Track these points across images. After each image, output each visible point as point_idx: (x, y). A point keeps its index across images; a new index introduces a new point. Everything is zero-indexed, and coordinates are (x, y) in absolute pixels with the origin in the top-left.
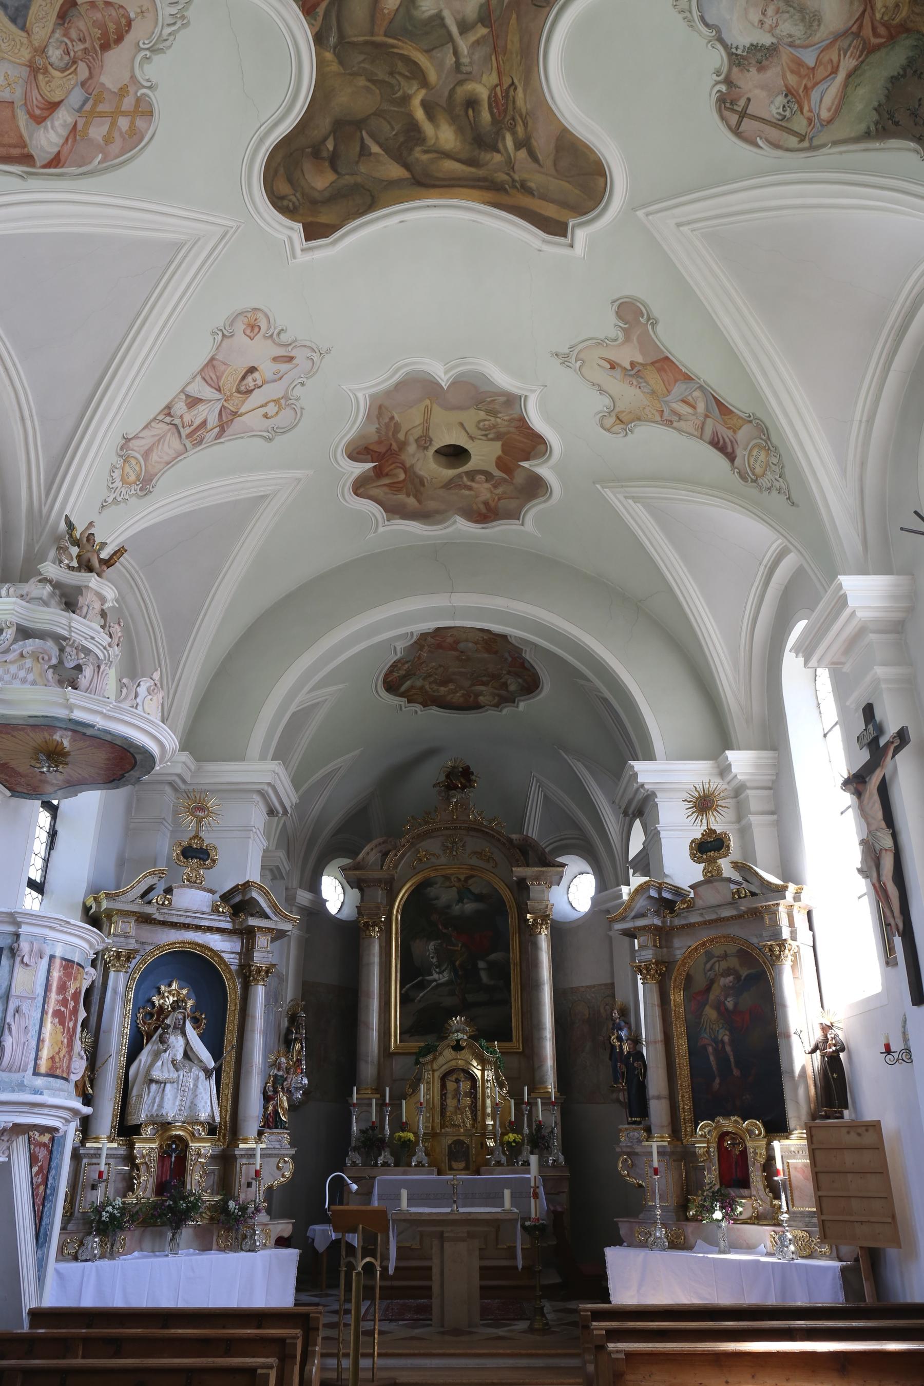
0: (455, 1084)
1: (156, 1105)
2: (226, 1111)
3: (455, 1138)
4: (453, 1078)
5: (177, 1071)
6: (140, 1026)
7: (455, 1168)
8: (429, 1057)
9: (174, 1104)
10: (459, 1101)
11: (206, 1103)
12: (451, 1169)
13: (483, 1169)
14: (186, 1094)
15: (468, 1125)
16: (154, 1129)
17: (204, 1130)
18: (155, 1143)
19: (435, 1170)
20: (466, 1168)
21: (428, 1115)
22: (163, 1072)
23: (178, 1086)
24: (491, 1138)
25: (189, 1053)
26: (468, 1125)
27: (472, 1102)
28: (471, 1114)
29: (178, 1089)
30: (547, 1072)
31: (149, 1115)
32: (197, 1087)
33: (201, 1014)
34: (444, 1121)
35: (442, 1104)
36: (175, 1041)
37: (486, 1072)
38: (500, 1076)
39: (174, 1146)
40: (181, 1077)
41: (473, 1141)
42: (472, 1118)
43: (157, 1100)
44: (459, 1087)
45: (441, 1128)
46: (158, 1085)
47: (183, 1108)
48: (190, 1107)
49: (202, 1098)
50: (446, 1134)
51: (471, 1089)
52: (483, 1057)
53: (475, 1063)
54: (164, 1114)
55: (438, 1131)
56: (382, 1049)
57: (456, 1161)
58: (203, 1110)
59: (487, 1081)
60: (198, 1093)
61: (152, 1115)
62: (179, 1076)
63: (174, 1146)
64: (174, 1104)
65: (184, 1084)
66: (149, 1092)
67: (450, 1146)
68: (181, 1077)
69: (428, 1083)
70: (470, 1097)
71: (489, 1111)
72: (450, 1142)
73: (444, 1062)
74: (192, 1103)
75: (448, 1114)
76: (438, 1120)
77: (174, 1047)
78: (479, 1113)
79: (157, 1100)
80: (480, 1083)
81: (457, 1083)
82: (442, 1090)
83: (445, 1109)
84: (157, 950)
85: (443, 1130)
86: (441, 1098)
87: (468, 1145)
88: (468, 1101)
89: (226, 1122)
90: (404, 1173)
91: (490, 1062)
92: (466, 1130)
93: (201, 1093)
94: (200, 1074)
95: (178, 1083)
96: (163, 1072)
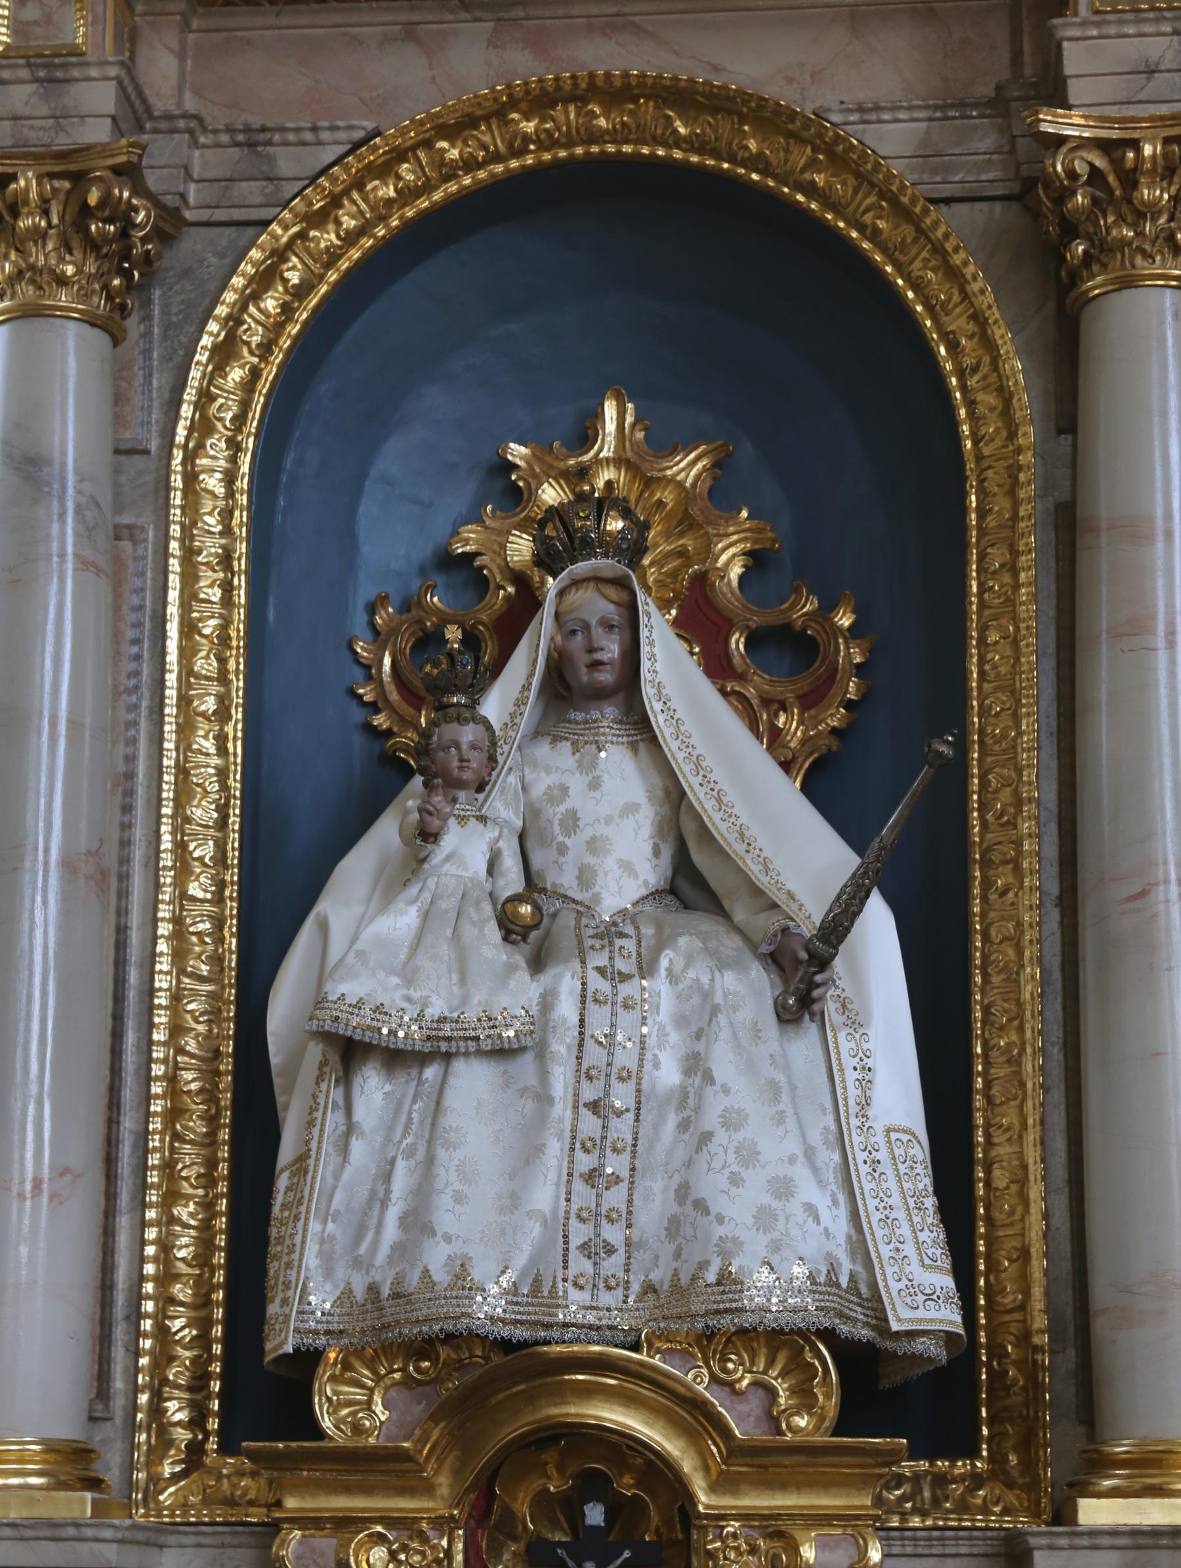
1: (393, 1214)
2: (1024, 1254)
5: (537, 964)
6: (380, 720)
9: (513, 1201)
11: (783, 1189)
14: (622, 1128)
16: (408, 1382)
17: (805, 1397)
18: (427, 1489)
22: (409, 975)
23: (544, 1075)
25: (699, 858)
29: (544, 1098)
31: (359, 1292)
32: (709, 1078)
33: (828, 608)
36: (577, 783)
39: (595, 1515)
40: (567, 1009)
43: (401, 1183)
46: (403, 1083)
47: (613, 1234)
48: (673, 1227)
49: (749, 1155)
54: (440, 1276)
58: (755, 1245)
60: (711, 1119)
61: (373, 1290)
62: (547, 1002)
63: (595, 1515)
64: (513, 1201)
65: (594, 1056)
66: (350, 1129)
68: (567, 1009)
74: (683, 1192)
77: (571, 822)
79: (401, 1183)
84: (385, 170)
89: (1024, 1338)
93: (733, 1120)
94: (729, 980)
95: (542, 1054)
96: (409, 975)
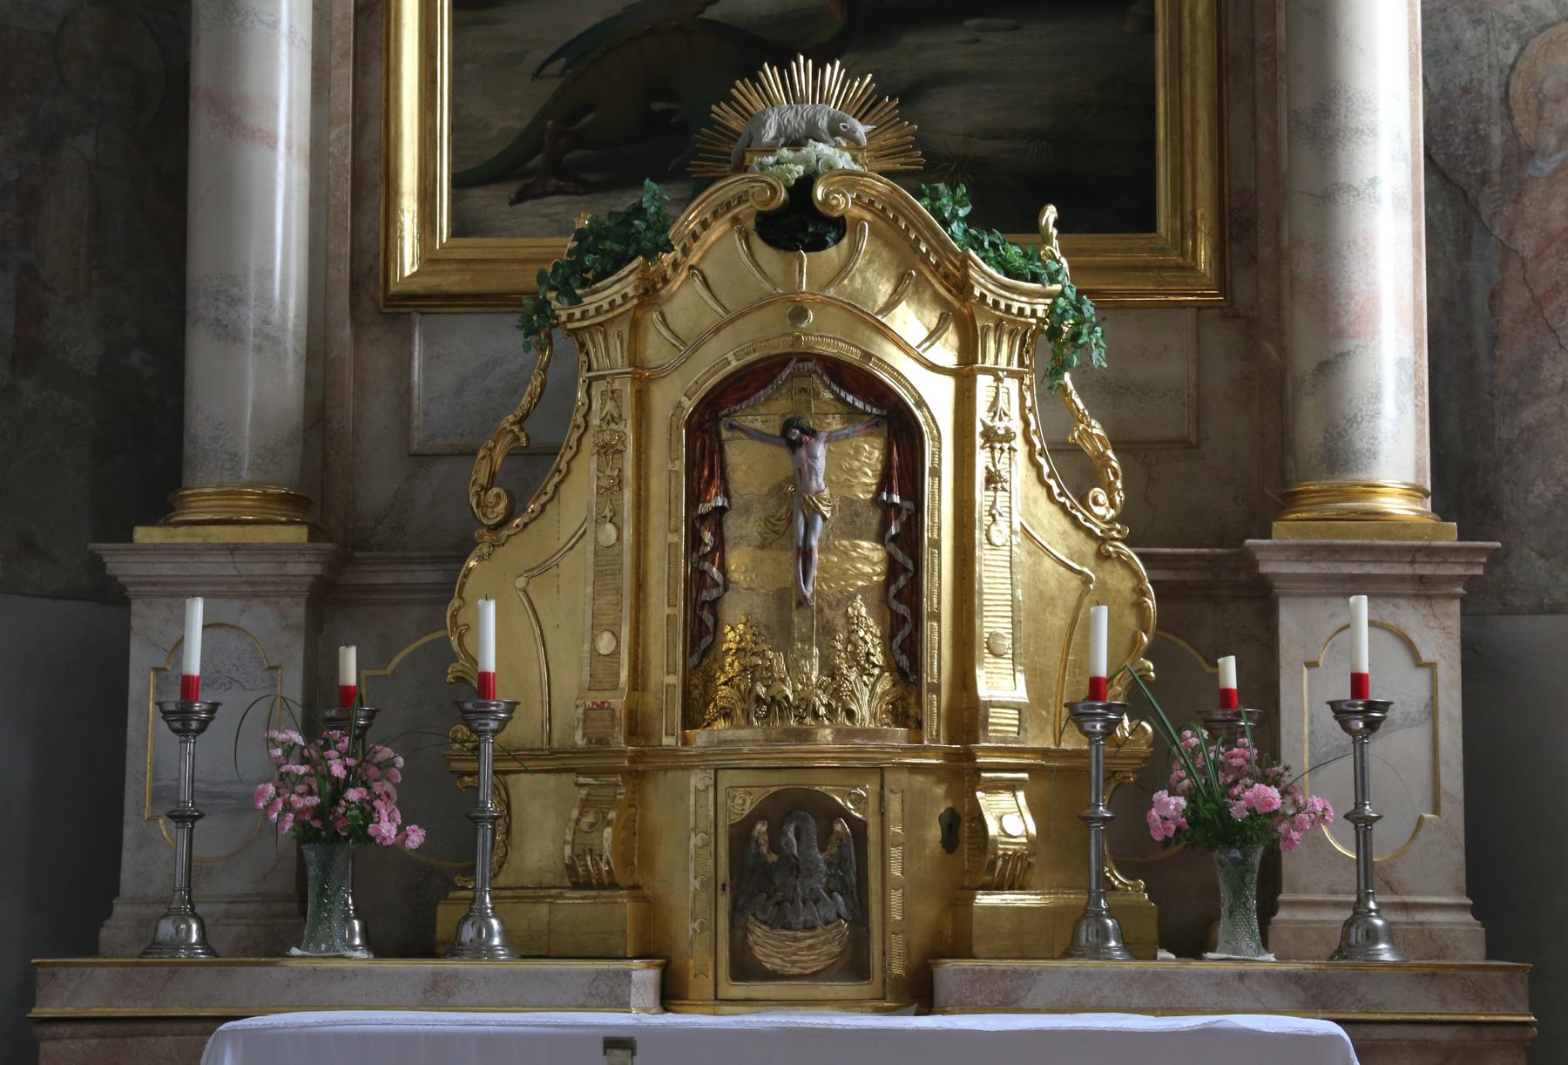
0: (782, 454)
3: (776, 782)
4: (762, 416)
7: (773, 962)
8: (621, 286)
10: (805, 554)
12: (745, 968)
13: (950, 970)
15: (865, 707)
19: (644, 976)
20: (854, 964)
21: (605, 644)
24: (1012, 787)
26: (865, 707)
27: (893, 568)
28: (888, 638)
30: (1376, 397)
34: (709, 680)
35: (697, 580)
37: (984, 384)
38: (1075, 417)
41: (895, 804)
42: (892, 666)
44: (801, 475)
45: (692, 717)
50: (719, 763)
51: (885, 482)
52: (962, 287)
53: (910, 321)
55: (667, 741)
56: (343, 272)
57: (780, 922)
59: (990, 436)
67: (741, 835)
69: (608, 451)
70: (880, 538)
71: (994, 620)
72: (743, 805)
73: (709, 321)
75: (731, 638)
76: (666, 677)
78: (939, 636)
80: (941, 454)
81: (794, 446)
82: (694, 498)
83: (714, 605)
85: (700, 737)
86: (694, 541)
87: (859, 828)
88: (869, 557)
90: (436, 995)
91: (1009, 325)
92: (852, 733)
